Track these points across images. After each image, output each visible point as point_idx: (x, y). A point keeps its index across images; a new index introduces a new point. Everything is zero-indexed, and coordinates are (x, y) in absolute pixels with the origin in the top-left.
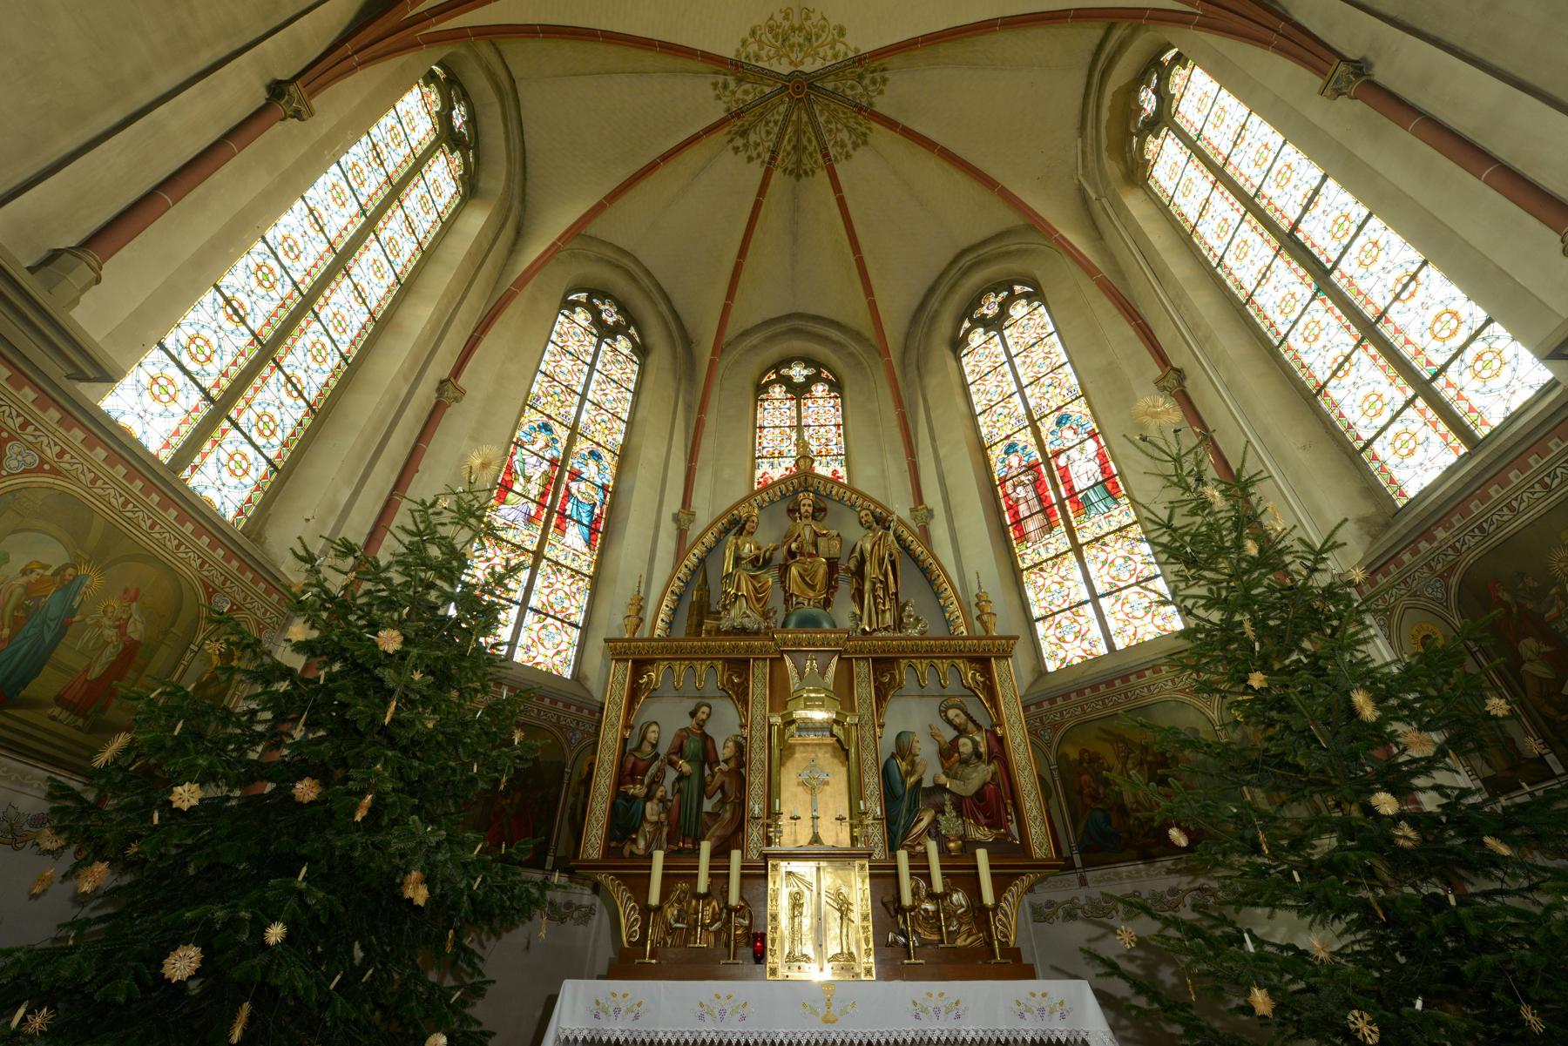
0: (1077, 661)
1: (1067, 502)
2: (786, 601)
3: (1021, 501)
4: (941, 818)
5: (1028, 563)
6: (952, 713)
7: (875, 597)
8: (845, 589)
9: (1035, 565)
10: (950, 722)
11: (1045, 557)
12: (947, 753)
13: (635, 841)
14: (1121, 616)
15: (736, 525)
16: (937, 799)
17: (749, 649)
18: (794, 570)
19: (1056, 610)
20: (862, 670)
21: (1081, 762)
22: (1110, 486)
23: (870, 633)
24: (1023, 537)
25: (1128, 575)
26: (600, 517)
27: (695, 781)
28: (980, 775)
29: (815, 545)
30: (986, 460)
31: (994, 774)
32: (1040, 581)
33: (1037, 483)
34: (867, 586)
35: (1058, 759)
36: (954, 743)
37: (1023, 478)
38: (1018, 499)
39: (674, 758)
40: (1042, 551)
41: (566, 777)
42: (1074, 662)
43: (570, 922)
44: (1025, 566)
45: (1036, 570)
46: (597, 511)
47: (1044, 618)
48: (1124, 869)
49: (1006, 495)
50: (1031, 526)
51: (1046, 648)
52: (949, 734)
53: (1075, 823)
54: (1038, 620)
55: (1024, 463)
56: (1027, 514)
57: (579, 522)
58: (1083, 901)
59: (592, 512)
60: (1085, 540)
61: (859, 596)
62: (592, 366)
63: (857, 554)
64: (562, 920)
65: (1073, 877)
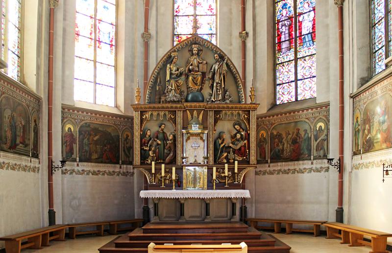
0: (286, 102)
1: (298, 38)
2: (187, 88)
3: (283, 33)
4: (229, 155)
5: (280, 62)
6: (236, 126)
7: (217, 89)
8: (207, 84)
9: (282, 63)
10: (236, 129)
11: (286, 60)
13: (148, 161)
14: (302, 88)
15: (169, 59)
16: (227, 150)
17: (176, 108)
18: (190, 78)
19: (284, 82)
20: (211, 114)
21: (277, 135)
22: (313, 35)
23: (214, 102)
24: (280, 50)
25: (308, 74)
27: (162, 146)
28: (241, 144)
29: (198, 67)
31: (245, 144)
32: (282, 70)
33: (290, 27)
34: (215, 84)
35: (271, 134)
36: (235, 135)
37: (286, 22)
38: (282, 32)
39: (156, 139)
40: (285, 57)
41: (120, 139)
42: (285, 102)
43: (128, 176)
44: (279, 63)
45: (281, 65)
47: (280, 84)
48: (279, 164)
49: (278, 29)
50: (284, 45)
51: (278, 96)
53: (271, 151)
54: (278, 85)
55: (287, 15)
56: (284, 40)
58: (268, 171)
60: (300, 57)
61: (212, 87)
63: (212, 70)
64: (126, 176)
65: (267, 165)
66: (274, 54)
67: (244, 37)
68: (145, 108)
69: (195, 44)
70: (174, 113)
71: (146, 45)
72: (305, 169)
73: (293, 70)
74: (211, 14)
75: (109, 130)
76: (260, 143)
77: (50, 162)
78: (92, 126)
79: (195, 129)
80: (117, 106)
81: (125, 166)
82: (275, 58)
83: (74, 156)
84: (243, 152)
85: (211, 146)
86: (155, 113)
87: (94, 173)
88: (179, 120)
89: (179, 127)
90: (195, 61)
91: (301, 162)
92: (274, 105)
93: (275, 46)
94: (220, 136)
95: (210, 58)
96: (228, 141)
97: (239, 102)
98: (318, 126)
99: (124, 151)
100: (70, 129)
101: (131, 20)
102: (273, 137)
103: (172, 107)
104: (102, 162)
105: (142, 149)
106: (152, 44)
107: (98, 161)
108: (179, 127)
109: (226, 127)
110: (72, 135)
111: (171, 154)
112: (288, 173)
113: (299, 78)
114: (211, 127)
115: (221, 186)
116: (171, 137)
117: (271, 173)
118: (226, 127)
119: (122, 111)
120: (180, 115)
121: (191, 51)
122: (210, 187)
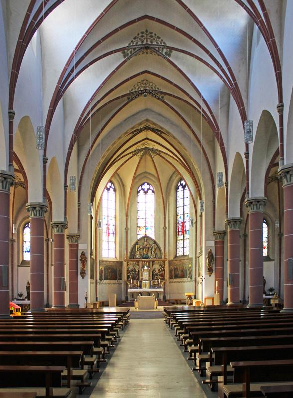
8: (150, 252)
12: (159, 270)
15: (136, 243)
20: (151, 262)
24: (179, 235)
28: (162, 272)
30: (177, 218)
50: (180, 233)
61: (152, 253)
66: (177, 236)
69: (146, 237)
70: (138, 262)
71: (127, 233)
76: (171, 271)
77: (96, 280)
79: (146, 268)
80: (115, 257)
82: (177, 238)
84: (163, 275)
85: (151, 274)
87: (109, 284)
90: (145, 243)
92: (176, 256)
93: (177, 233)
94: (154, 270)
95: (151, 242)
96: (157, 272)
97: (161, 258)
101: (121, 223)
102: (175, 269)
105: (127, 275)
106: (129, 232)
107: (110, 279)
109: (157, 267)
115: (154, 287)
117: (175, 282)
118: (157, 267)
119: (118, 259)
120: (140, 263)
121: (144, 240)
122: (151, 288)
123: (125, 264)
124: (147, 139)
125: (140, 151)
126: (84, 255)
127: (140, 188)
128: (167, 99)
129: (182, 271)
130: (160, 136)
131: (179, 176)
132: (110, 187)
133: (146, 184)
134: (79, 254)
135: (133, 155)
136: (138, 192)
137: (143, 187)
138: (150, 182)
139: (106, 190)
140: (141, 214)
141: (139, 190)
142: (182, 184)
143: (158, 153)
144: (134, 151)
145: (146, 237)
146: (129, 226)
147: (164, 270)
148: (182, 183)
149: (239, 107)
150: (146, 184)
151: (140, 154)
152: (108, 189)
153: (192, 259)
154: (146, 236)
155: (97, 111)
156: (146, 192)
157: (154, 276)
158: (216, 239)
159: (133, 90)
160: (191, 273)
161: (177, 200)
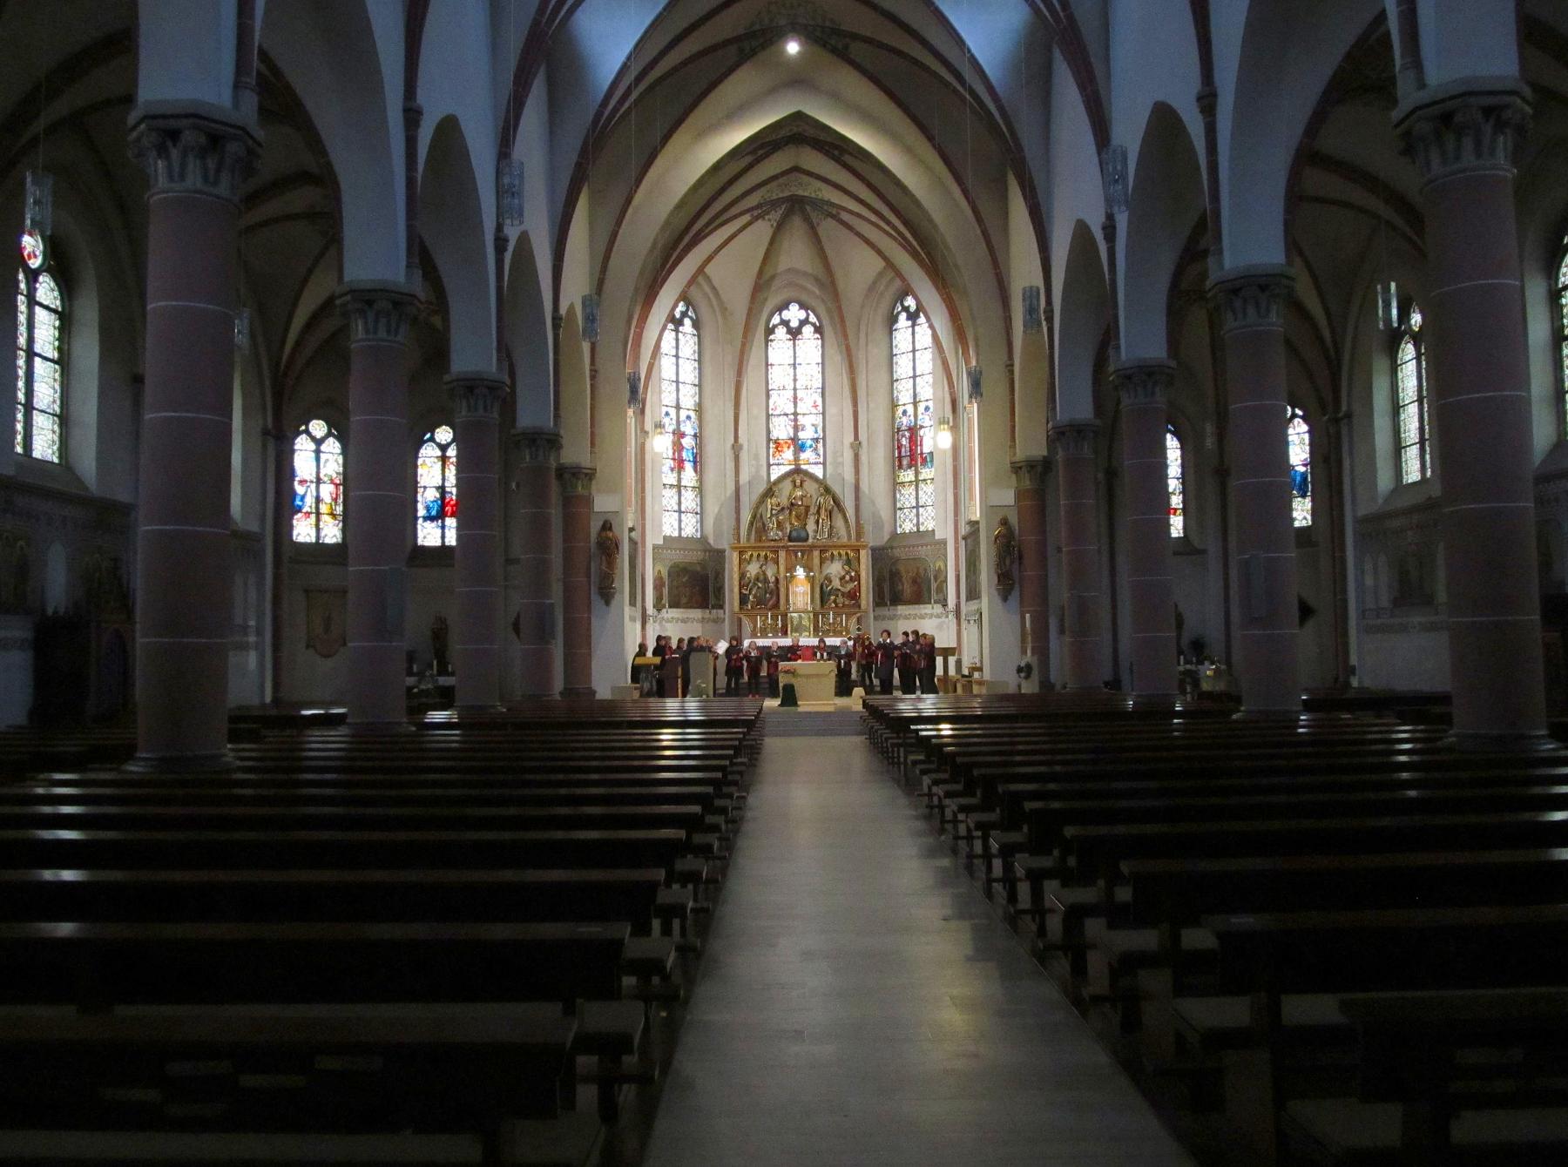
12: (842, 578)
15: (769, 492)
20: (816, 553)
24: (900, 467)
26: (696, 453)
28: (850, 586)
34: (821, 521)
36: (844, 577)
46: (695, 451)
49: (898, 440)
50: (905, 462)
52: (843, 573)
57: (689, 461)
59: (693, 453)
62: (677, 356)
67: (856, 446)
68: (745, 547)
69: (797, 474)
71: (737, 459)
72: (925, 614)
73: (914, 493)
74: (816, 412)
75: (699, 568)
78: (681, 566)
81: (715, 611)
82: (894, 477)
83: (663, 602)
84: (854, 596)
86: (755, 554)
88: (782, 561)
89: (782, 568)
91: (922, 606)
93: (897, 463)
96: (836, 583)
98: (937, 565)
99: (714, 592)
100: (659, 572)
103: (773, 547)
104: (691, 607)
105: (740, 593)
106: (744, 456)
107: (689, 606)
108: (782, 568)
109: (835, 569)
110: (661, 578)
111: (774, 598)
112: (909, 619)
113: (920, 504)
114: (816, 567)
116: (773, 579)
120: (782, 554)
123: (733, 560)
124: (796, 169)
125: (774, 204)
126: (610, 529)
127: (776, 320)
128: (857, 50)
129: (914, 581)
130: (838, 160)
131: (898, 283)
132: (684, 314)
133: (794, 307)
134: (595, 527)
135: (756, 218)
136: (770, 331)
137: (786, 315)
138: (804, 297)
139: (671, 326)
140: (780, 402)
141: (775, 326)
142: (906, 309)
143: (832, 211)
144: (759, 206)
145: (797, 474)
146: (742, 439)
147: (858, 578)
148: (906, 304)
149: (1082, 87)
150: (794, 307)
151: (776, 215)
152: (678, 323)
153: (944, 543)
154: (798, 471)
155: (651, 88)
156: (794, 333)
157: (823, 594)
158: (1018, 480)
159: (757, 27)
160: (942, 589)
161: (892, 356)
